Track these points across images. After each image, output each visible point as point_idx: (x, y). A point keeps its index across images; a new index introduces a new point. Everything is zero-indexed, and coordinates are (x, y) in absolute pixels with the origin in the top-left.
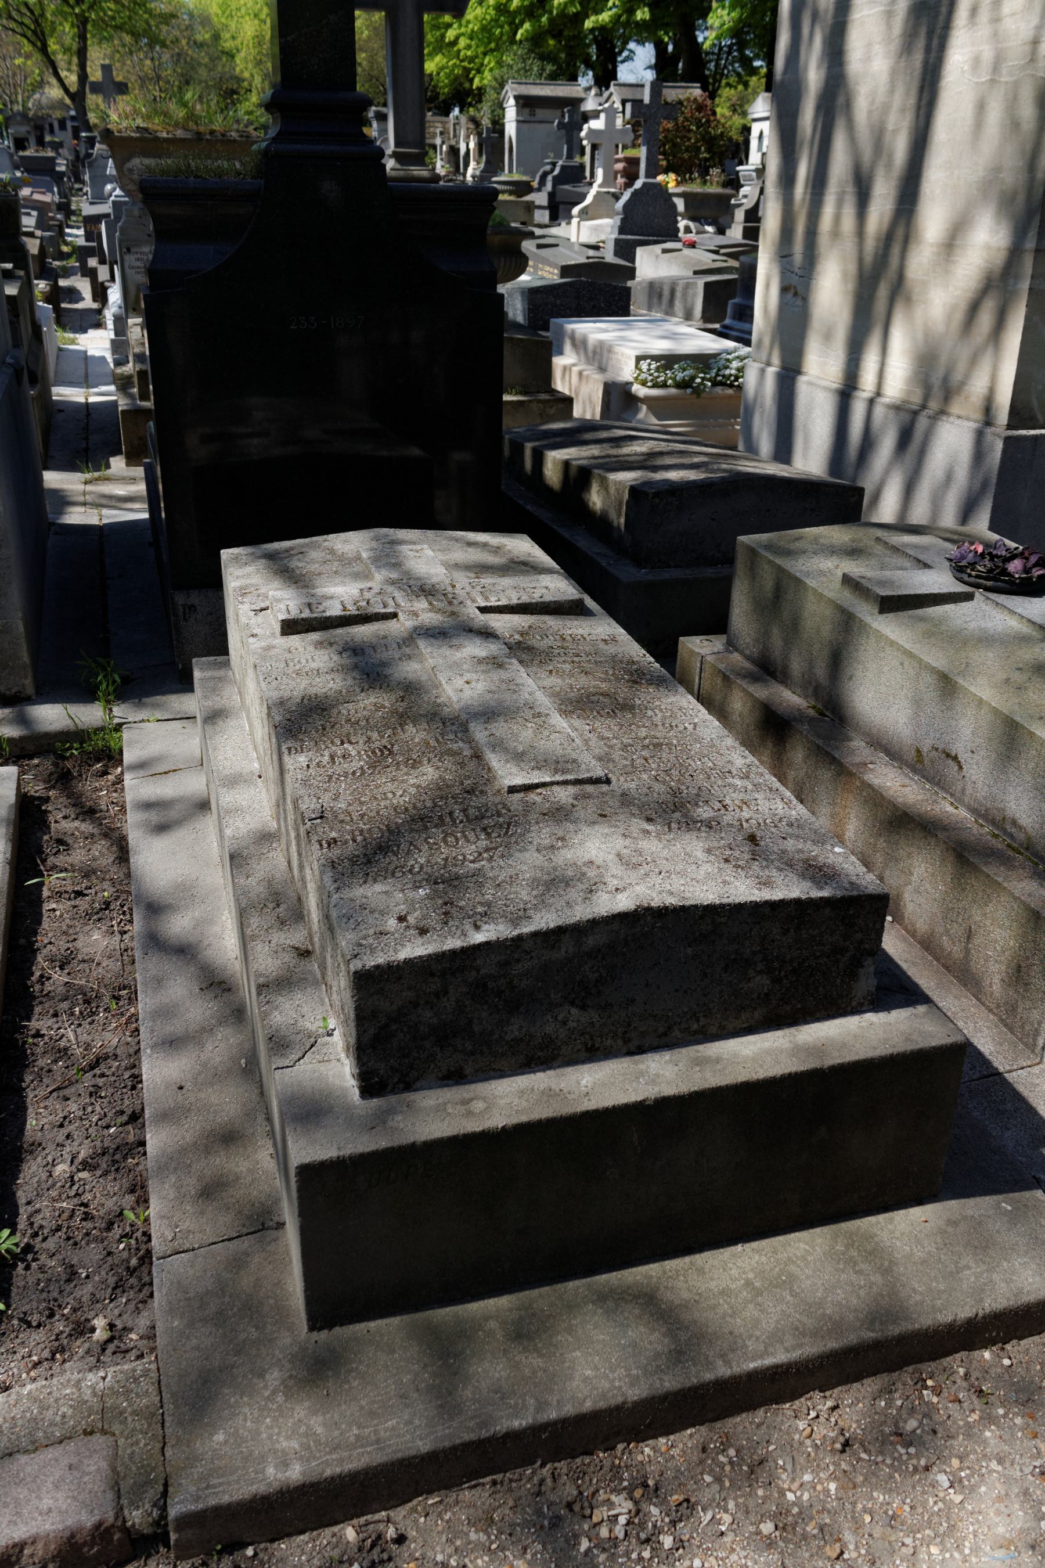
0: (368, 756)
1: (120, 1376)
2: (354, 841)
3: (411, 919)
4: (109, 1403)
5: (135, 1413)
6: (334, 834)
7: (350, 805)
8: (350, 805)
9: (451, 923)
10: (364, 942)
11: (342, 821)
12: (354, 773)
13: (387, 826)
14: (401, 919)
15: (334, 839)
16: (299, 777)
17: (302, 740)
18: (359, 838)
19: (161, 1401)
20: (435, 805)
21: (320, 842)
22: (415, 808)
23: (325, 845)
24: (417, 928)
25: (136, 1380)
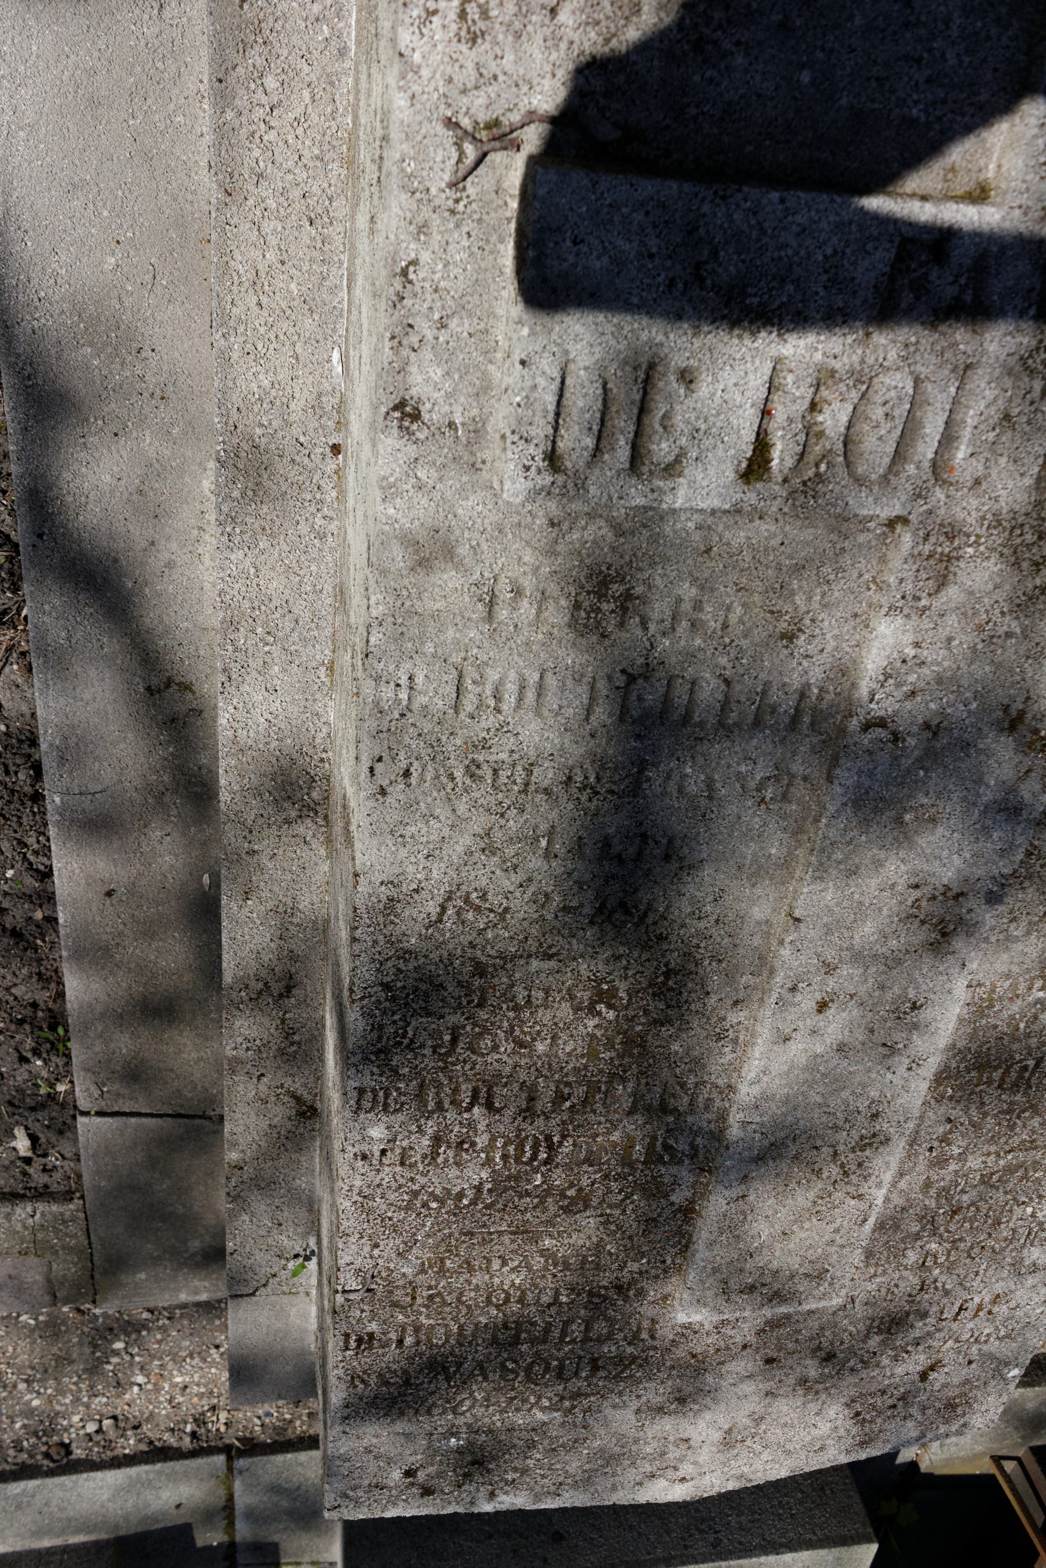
0: (505, 1157)
1: (49, 1217)
2: (400, 1342)
3: (421, 1475)
4: (40, 1236)
5: (63, 1248)
6: (373, 1327)
7: (423, 1271)
8: (423, 1271)
9: (466, 1487)
10: (351, 1493)
11: (395, 1305)
12: (461, 1195)
13: (461, 1328)
14: (409, 1473)
15: (371, 1335)
16: (358, 1183)
17: (395, 1071)
18: (409, 1340)
19: (90, 1243)
20: (556, 1301)
21: (347, 1336)
22: (521, 1301)
23: (353, 1344)
24: (423, 1488)
25: (64, 1222)
